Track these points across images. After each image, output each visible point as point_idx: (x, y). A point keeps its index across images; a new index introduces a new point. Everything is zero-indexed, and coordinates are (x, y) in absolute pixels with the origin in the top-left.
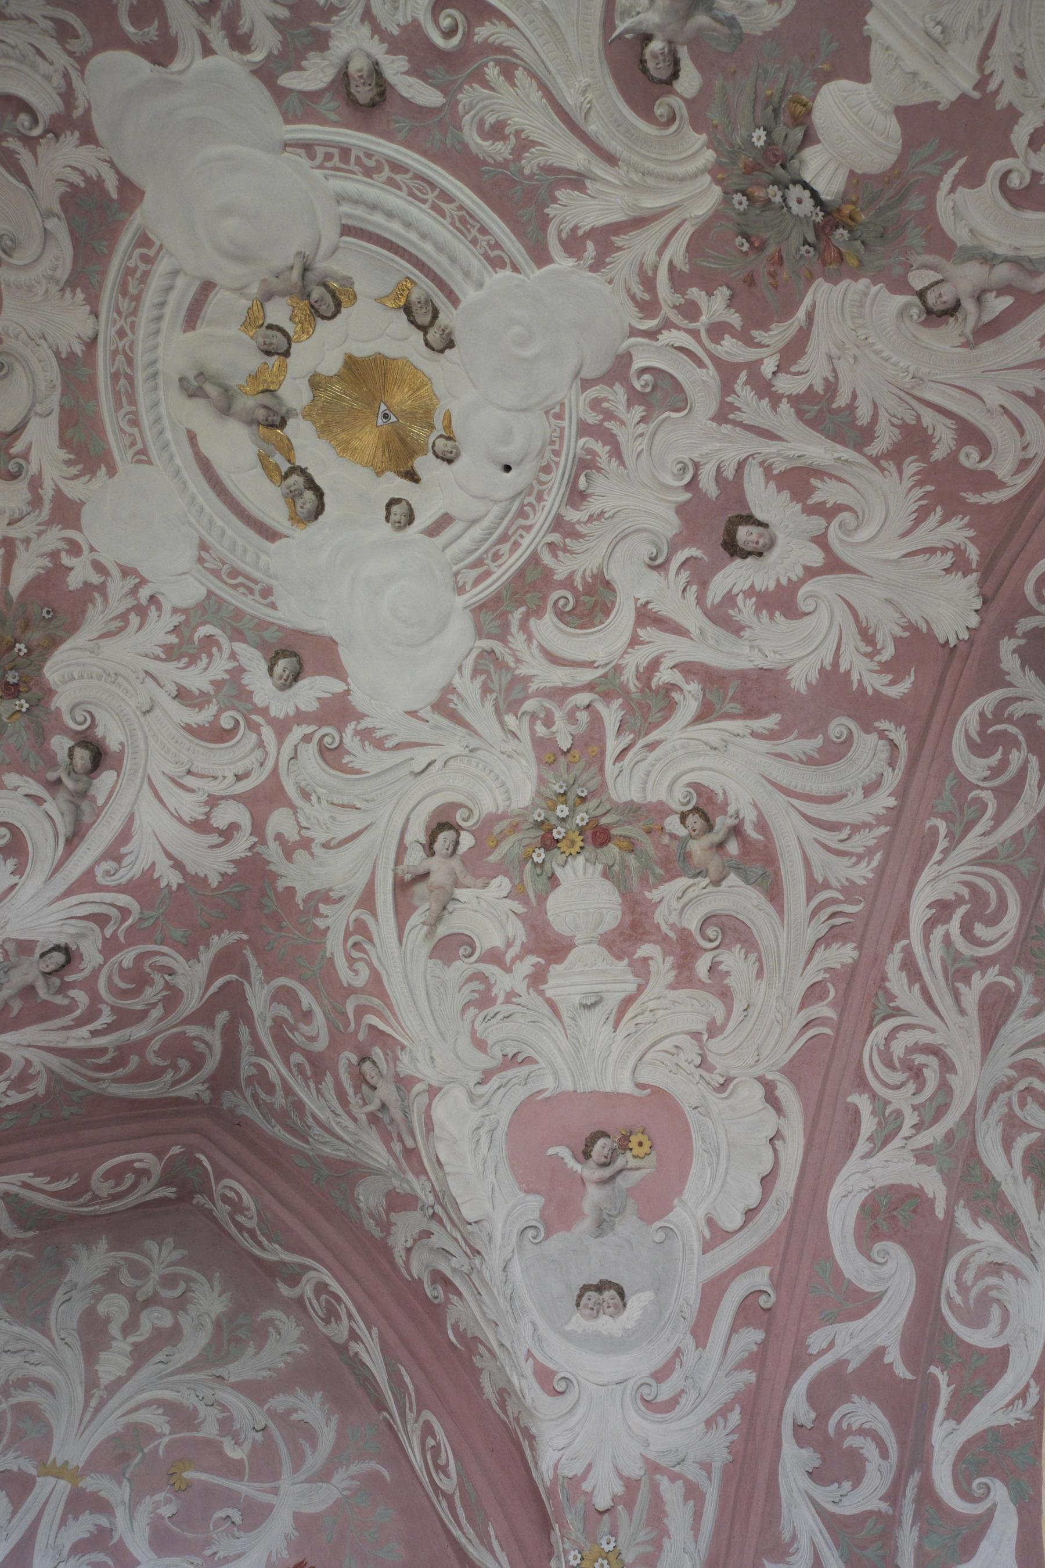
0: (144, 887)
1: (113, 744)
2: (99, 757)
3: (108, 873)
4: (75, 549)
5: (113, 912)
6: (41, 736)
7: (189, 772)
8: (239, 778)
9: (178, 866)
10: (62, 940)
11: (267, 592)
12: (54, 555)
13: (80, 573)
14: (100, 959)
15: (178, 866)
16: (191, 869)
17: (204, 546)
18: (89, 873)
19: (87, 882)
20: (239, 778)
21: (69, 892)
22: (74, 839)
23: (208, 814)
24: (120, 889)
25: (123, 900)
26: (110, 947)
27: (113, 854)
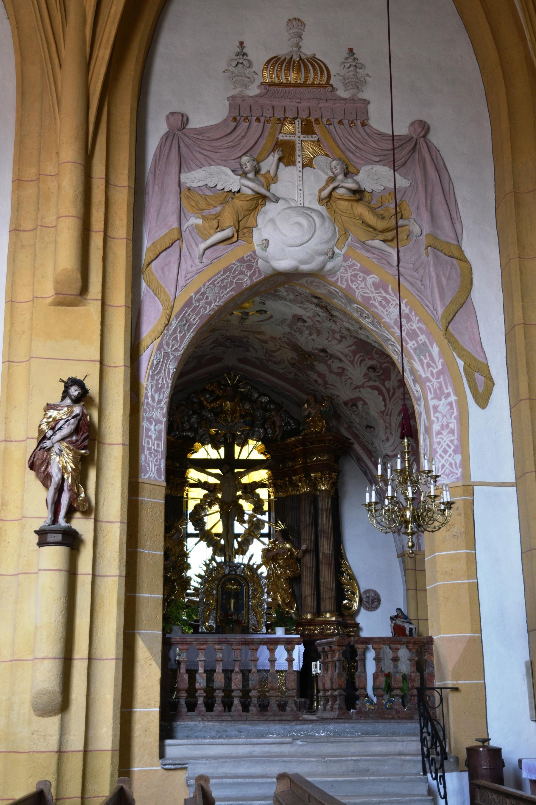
0: (355, 353)
1: (322, 347)
2: (324, 350)
3: (350, 357)
4: (280, 339)
5: (361, 358)
6: (320, 356)
7: (327, 339)
8: (328, 333)
9: (350, 346)
10: (366, 368)
11: (285, 319)
12: (282, 342)
13: (285, 339)
14: (375, 361)
15: (350, 346)
16: (352, 344)
17: (277, 324)
18: (349, 361)
19: (352, 362)
20: (328, 333)
21: (354, 365)
22: (341, 360)
23: (337, 340)
24: (354, 357)
25: (358, 356)
26: (372, 359)
27: (346, 356)
